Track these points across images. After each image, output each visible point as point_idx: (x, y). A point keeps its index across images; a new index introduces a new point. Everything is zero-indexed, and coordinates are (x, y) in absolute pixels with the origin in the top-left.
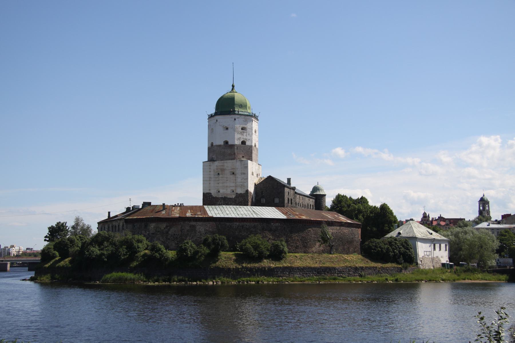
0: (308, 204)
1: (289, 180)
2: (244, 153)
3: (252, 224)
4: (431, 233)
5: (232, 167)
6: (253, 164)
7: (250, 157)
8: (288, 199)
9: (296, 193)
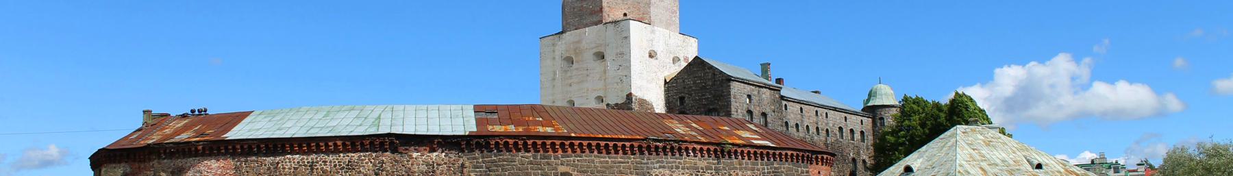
0: (841, 129)
1: (765, 68)
2: (626, 7)
3: (344, 158)
4: (1036, 163)
5: (598, 42)
6: (653, 32)
7: (643, 14)
8: (750, 112)
9: (782, 98)
